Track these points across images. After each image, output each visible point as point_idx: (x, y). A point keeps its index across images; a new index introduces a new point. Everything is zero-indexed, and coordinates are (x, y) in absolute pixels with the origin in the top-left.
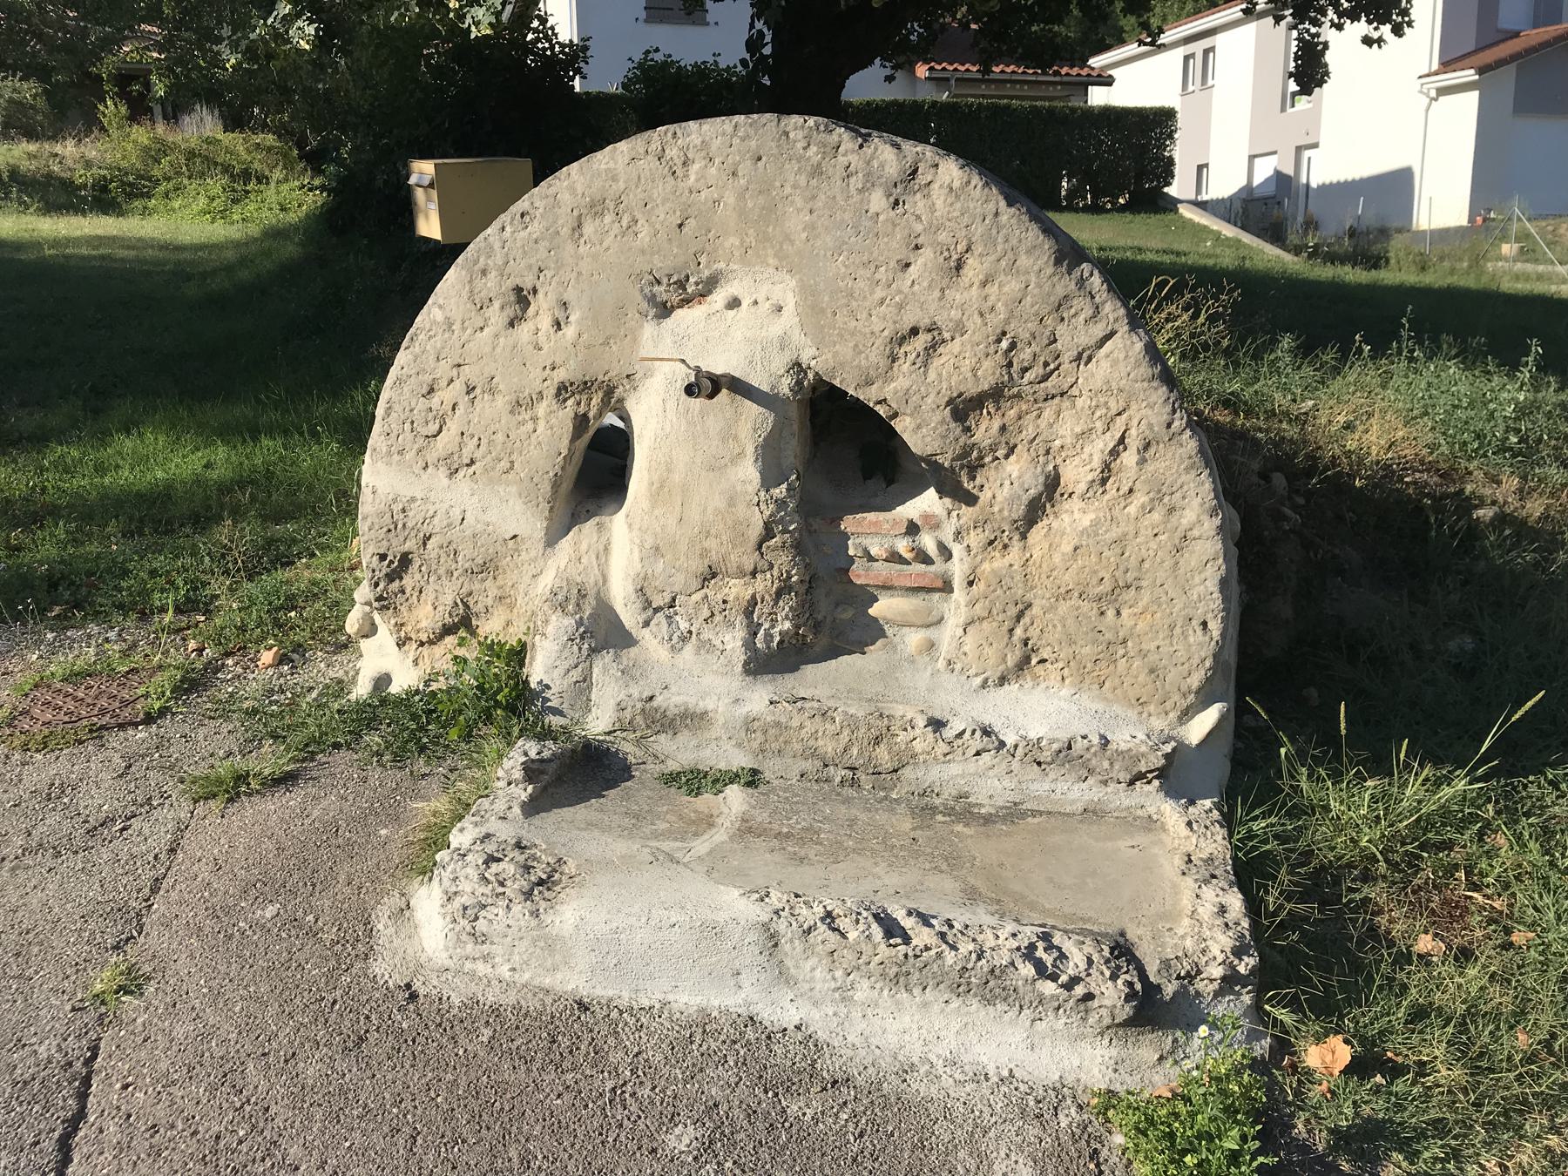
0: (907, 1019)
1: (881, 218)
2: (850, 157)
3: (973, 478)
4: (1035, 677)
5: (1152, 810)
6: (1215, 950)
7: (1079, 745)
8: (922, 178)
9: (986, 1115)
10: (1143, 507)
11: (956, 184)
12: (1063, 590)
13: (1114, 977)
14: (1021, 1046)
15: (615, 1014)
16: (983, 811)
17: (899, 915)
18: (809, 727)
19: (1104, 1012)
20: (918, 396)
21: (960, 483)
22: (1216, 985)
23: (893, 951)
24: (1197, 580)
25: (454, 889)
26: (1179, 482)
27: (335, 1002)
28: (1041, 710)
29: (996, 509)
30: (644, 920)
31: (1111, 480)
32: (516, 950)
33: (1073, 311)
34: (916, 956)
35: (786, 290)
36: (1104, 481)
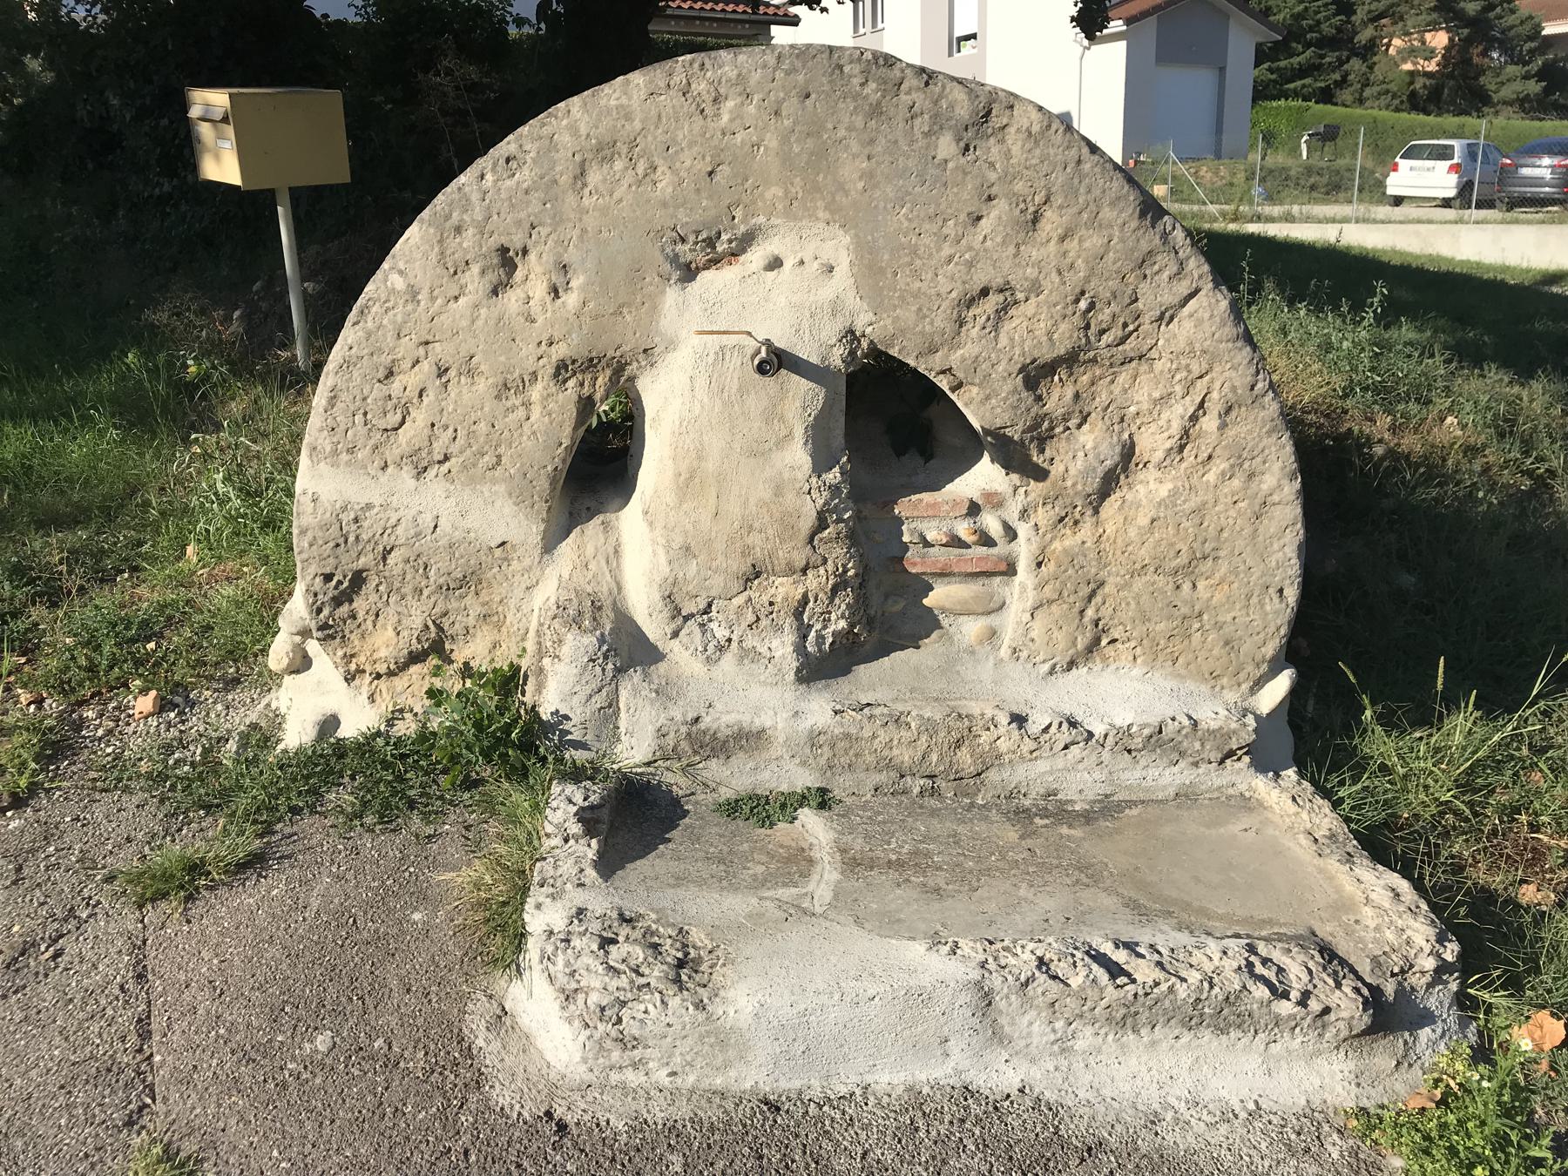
0: (1134, 1061)
1: (950, 165)
2: (914, 95)
3: (1042, 451)
4: (1105, 659)
5: (1242, 787)
6: (1419, 940)
7: (1171, 728)
8: (996, 122)
9: (1257, 1159)
10: (1223, 473)
11: (1036, 128)
12: (1138, 566)
13: (1338, 985)
14: (1259, 1072)
15: (812, 1109)
16: (1077, 808)
17: (1107, 948)
18: (883, 737)
19: (1341, 1025)
20: (988, 363)
21: (1028, 457)
22: (1428, 978)
23: (1121, 993)
24: (1276, 546)
25: (574, 985)
26: (1261, 446)
27: (466, 1153)
28: (1121, 694)
29: (1069, 483)
30: (837, 997)
31: (1188, 447)
32: (677, 1051)
33: (1156, 267)
34: (1147, 994)
35: (838, 247)
36: (1181, 448)
